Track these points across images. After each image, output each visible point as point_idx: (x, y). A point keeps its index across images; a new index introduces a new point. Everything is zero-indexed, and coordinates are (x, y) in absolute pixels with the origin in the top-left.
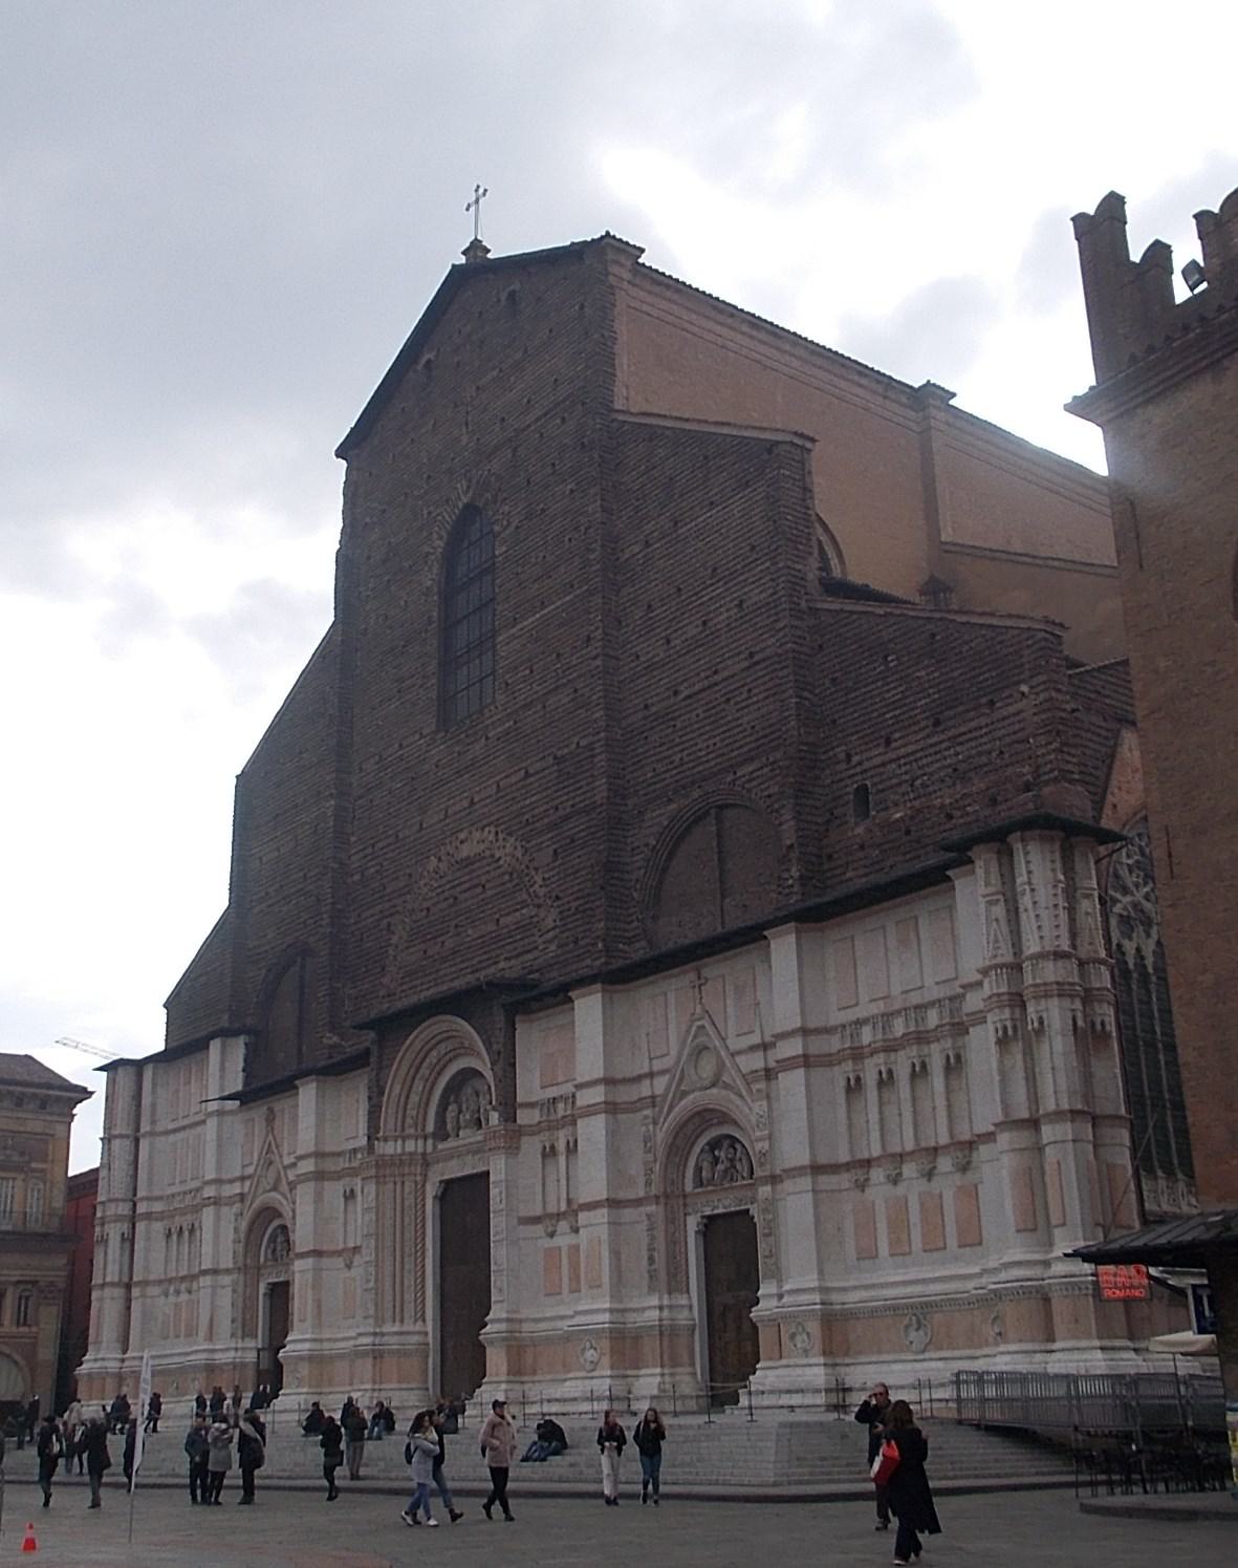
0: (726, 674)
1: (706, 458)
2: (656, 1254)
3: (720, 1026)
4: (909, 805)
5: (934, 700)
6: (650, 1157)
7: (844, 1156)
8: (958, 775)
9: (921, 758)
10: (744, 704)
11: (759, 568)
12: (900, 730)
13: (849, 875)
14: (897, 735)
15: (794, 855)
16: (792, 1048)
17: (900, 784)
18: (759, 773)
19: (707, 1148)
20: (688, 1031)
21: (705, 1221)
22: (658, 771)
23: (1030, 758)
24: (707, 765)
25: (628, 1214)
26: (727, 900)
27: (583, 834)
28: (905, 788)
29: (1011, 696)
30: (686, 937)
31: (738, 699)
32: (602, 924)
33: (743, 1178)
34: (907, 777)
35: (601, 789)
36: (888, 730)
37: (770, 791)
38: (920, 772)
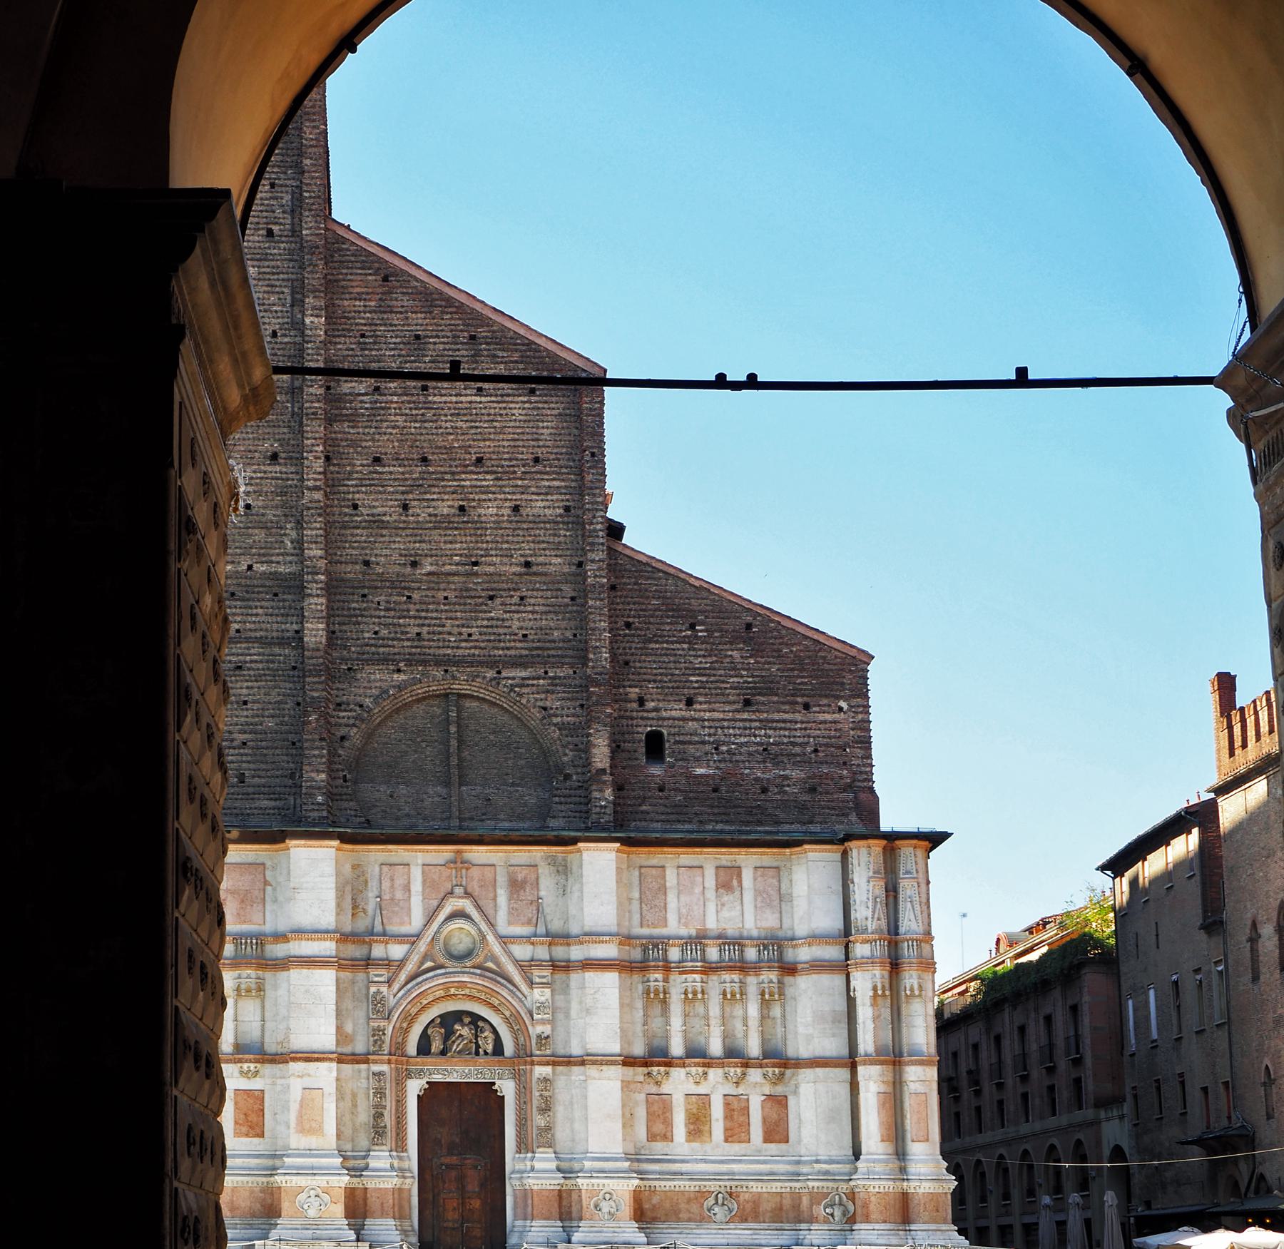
0: (492, 569)
1: (473, 338)
2: (386, 1113)
3: (490, 912)
4: (711, 764)
5: (749, 683)
7: (639, 1049)
8: (767, 753)
9: (728, 728)
10: (513, 608)
11: (547, 483)
12: (706, 695)
13: (644, 808)
14: (701, 699)
15: (608, 778)
16: (608, 950)
17: (704, 743)
18: (535, 682)
19: (438, 1020)
20: (439, 908)
21: (427, 1086)
22: (384, 632)
23: (845, 763)
24: (460, 652)
25: (347, 1068)
26: (464, 788)
27: (260, 666)
28: (707, 747)
29: (830, 706)
30: (399, 810)
31: (508, 600)
32: (323, 776)
33: (486, 1053)
34: (712, 739)
35: (315, 632)
36: (692, 692)
37: (548, 704)
38: (723, 738)
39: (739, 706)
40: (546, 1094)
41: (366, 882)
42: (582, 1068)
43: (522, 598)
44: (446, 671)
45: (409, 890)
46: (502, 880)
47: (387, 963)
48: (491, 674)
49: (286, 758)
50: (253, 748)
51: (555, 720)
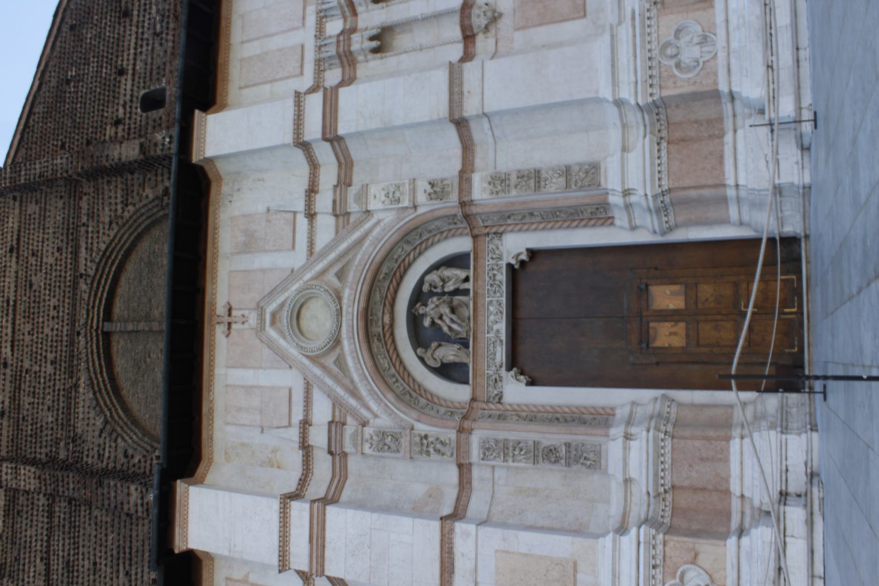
6: (405, 442)
19: (419, 350)
32: (133, 488)
33: (467, 279)
37: (107, 220)
39: (128, 20)
40: (514, 179)
41: (243, 444)
42: (473, 125)
43: (33, 255)
44: (79, 334)
45: (252, 387)
46: (245, 262)
47: (336, 425)
48: (83, 286)
49: (140, 526)
50: (130, 565)
51: (119, 211)
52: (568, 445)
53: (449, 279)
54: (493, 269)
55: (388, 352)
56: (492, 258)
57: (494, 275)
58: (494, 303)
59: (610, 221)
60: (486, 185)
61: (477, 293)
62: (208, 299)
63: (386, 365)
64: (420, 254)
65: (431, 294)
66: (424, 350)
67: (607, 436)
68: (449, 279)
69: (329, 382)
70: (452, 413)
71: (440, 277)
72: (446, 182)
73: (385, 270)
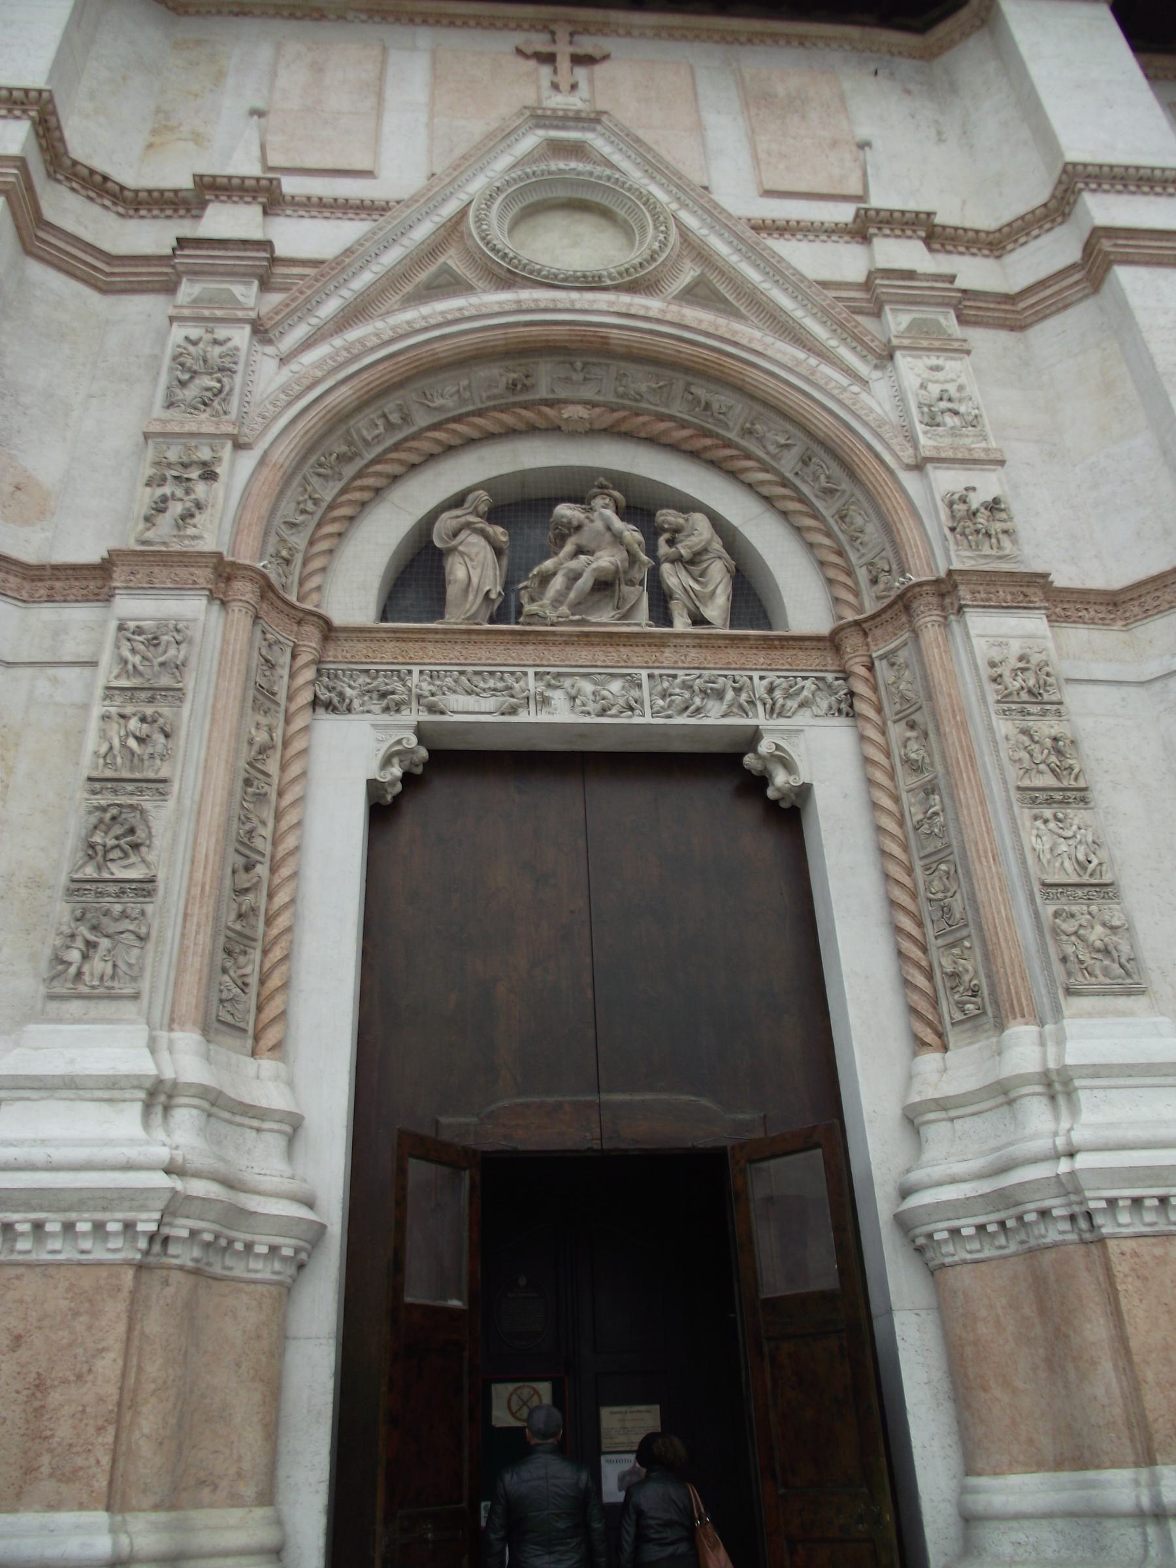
40: (1046, 728)
52: (146, 887)
53: (700, 577)
54: (738, 691)
55: (480, 413)
56: (771, 690)
57: (720, 695)
58: (635, 693)
59: (929, 1036)
60: (1016, 647)
61: (664, 645)
62: (618, 17)
63: (439, 402)
64: (768, 500)
65: (652, 532)
66: (483, 508)
67: (172, 1023)
68: (700, 577)
69: (392, 257)
70: (288, 562)
71: (705, 550)
72: (1006, 542)
73: (721, 399)
